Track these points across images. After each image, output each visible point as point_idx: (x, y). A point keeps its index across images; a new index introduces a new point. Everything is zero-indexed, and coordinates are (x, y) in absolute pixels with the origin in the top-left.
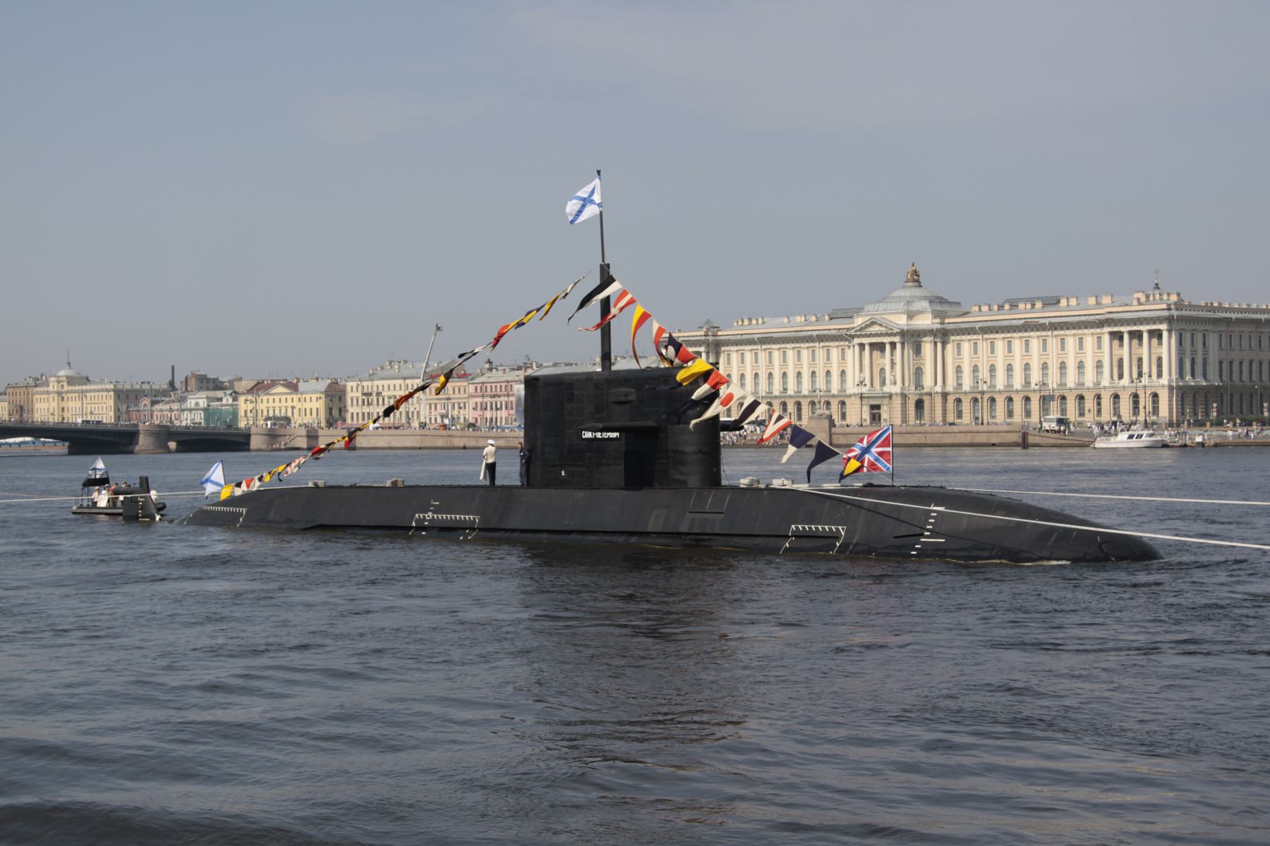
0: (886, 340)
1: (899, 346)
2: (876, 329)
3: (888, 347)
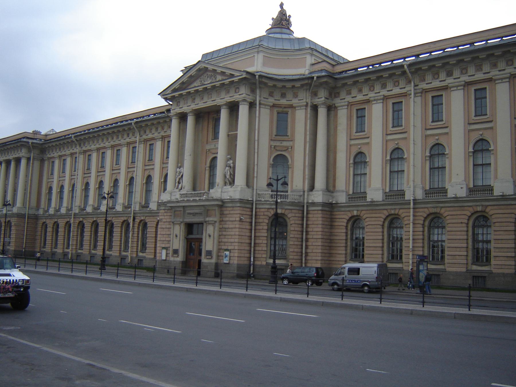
0: (221, 99)
1: (243, 110)
2: (208, 82)
3: (224, 114)
